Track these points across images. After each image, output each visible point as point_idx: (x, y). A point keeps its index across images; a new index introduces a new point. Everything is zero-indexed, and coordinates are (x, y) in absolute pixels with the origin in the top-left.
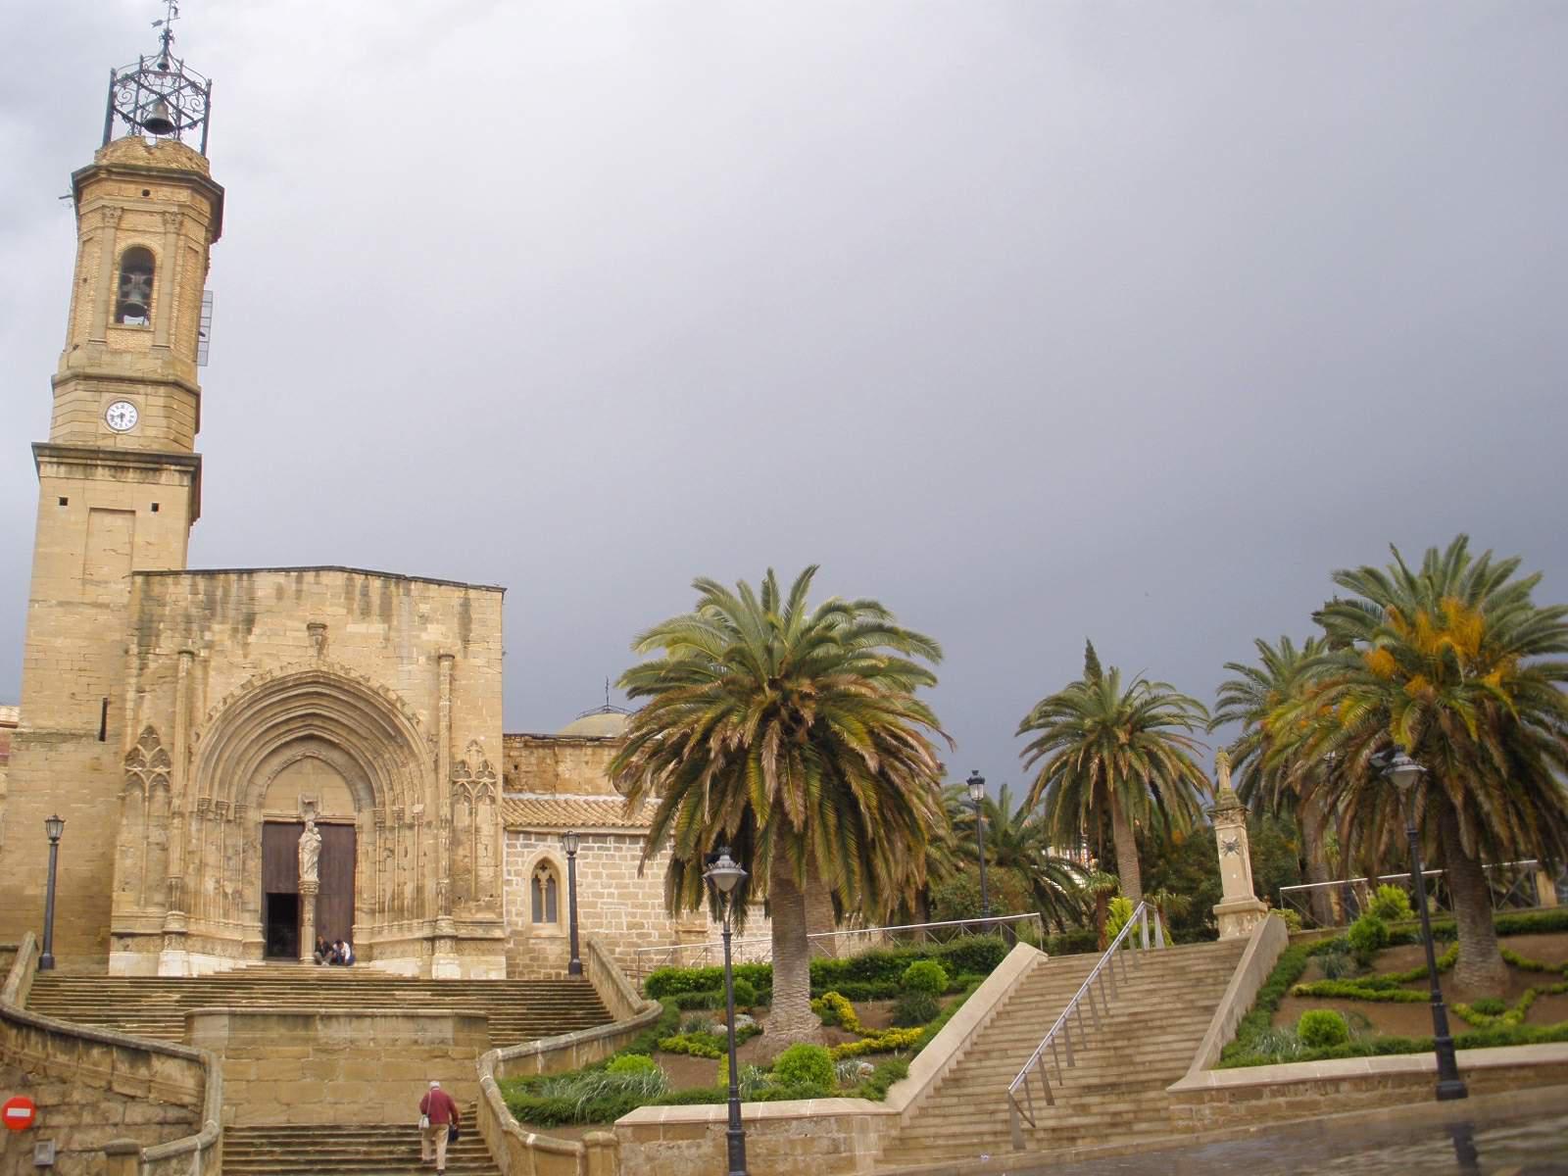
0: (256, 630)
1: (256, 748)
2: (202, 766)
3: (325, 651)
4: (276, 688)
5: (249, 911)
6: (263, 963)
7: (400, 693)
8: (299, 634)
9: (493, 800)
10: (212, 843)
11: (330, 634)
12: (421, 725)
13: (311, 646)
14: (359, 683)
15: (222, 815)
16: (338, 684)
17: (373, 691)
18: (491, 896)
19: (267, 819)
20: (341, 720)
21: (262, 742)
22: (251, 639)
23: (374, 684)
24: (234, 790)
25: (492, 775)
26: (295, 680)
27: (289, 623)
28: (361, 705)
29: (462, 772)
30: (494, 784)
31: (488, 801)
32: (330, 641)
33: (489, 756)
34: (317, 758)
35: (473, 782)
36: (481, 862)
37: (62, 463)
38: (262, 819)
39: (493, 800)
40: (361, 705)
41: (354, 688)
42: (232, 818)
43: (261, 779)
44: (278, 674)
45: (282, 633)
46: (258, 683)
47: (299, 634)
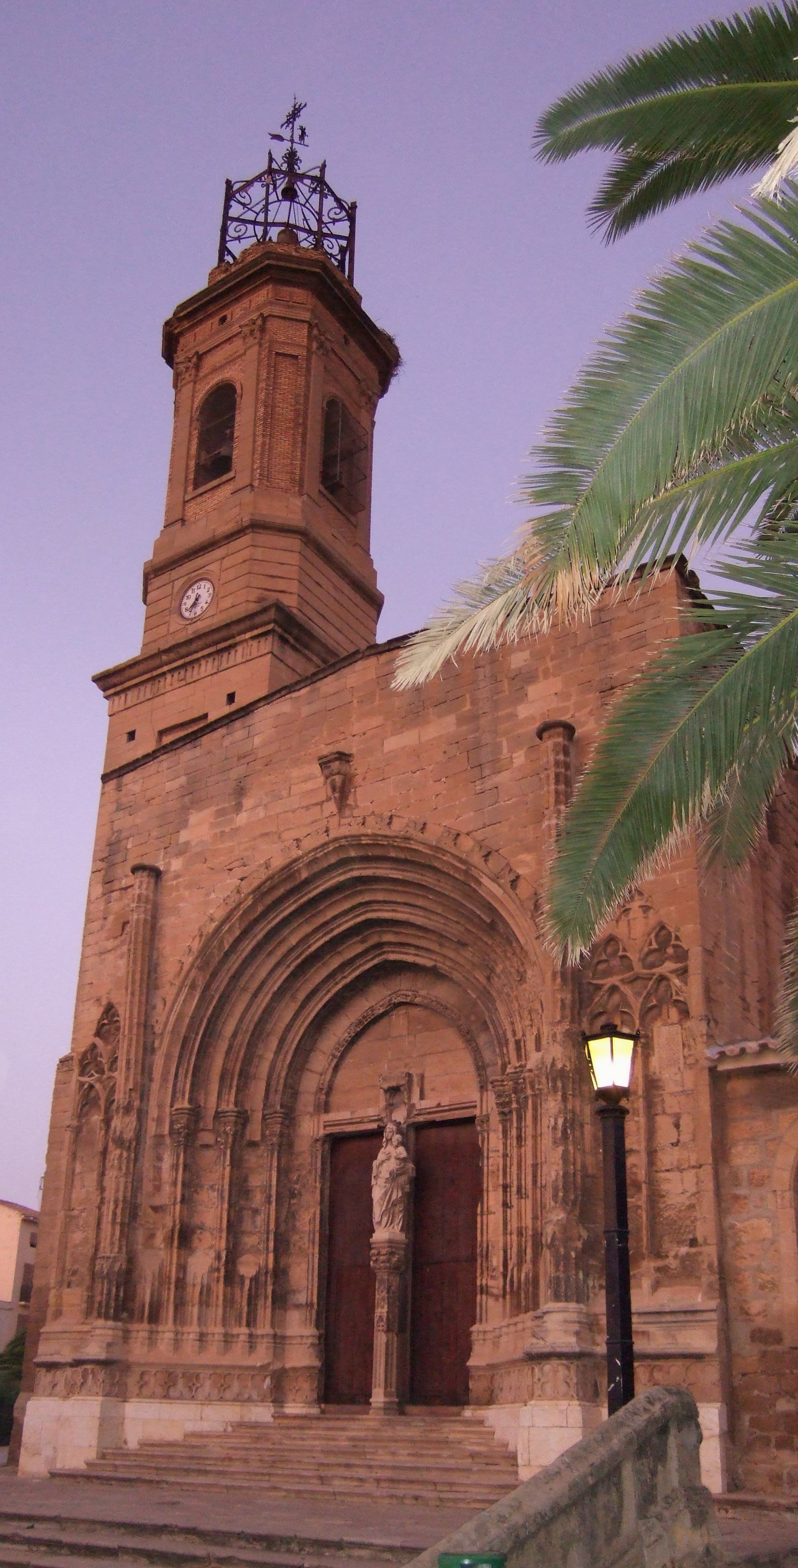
0: (248, 803)
1: (294, 1006)
2: (176, 1053)
3: (350, 801)
4: (281, 891)
5: (298, 1306)
6: (315, 1411)
7: (479, 835)
8: (310, 785)
9: (685, 1013)
10: (212, 1187)
11: (358, 767)
12: (522, 885)
13: (329, 799)
14: (407, 839)
15: (225, 1132)
16: (378, 852)
17: (431, 847)
18: (693, 1242)
19: (330, 1130)
20: (412, 919)
21: (301, 996)
22: (242, 819)
23: (433, 835)
24: (258, 1089)
25: (682, 955)
26: (309, 865)
27: (295, 773)
28: (428, 879)
29: (615, 962)
30: (683, 973)
31: (674, 1013)
32: (358, 780)
33: (668, 914)
34: (411, 1004)
35: (637, 978)
36: (667, 1158)
37: (129, 688)
38: (322, 1132)
39: (685, 1013)
40: (428, 879)
41: (402, 849)
42: (258, 1138)
43: (320, 1061)
44: (278, 862)
45: (284, 793)
46: (247, 888)
47: (310, 785)
